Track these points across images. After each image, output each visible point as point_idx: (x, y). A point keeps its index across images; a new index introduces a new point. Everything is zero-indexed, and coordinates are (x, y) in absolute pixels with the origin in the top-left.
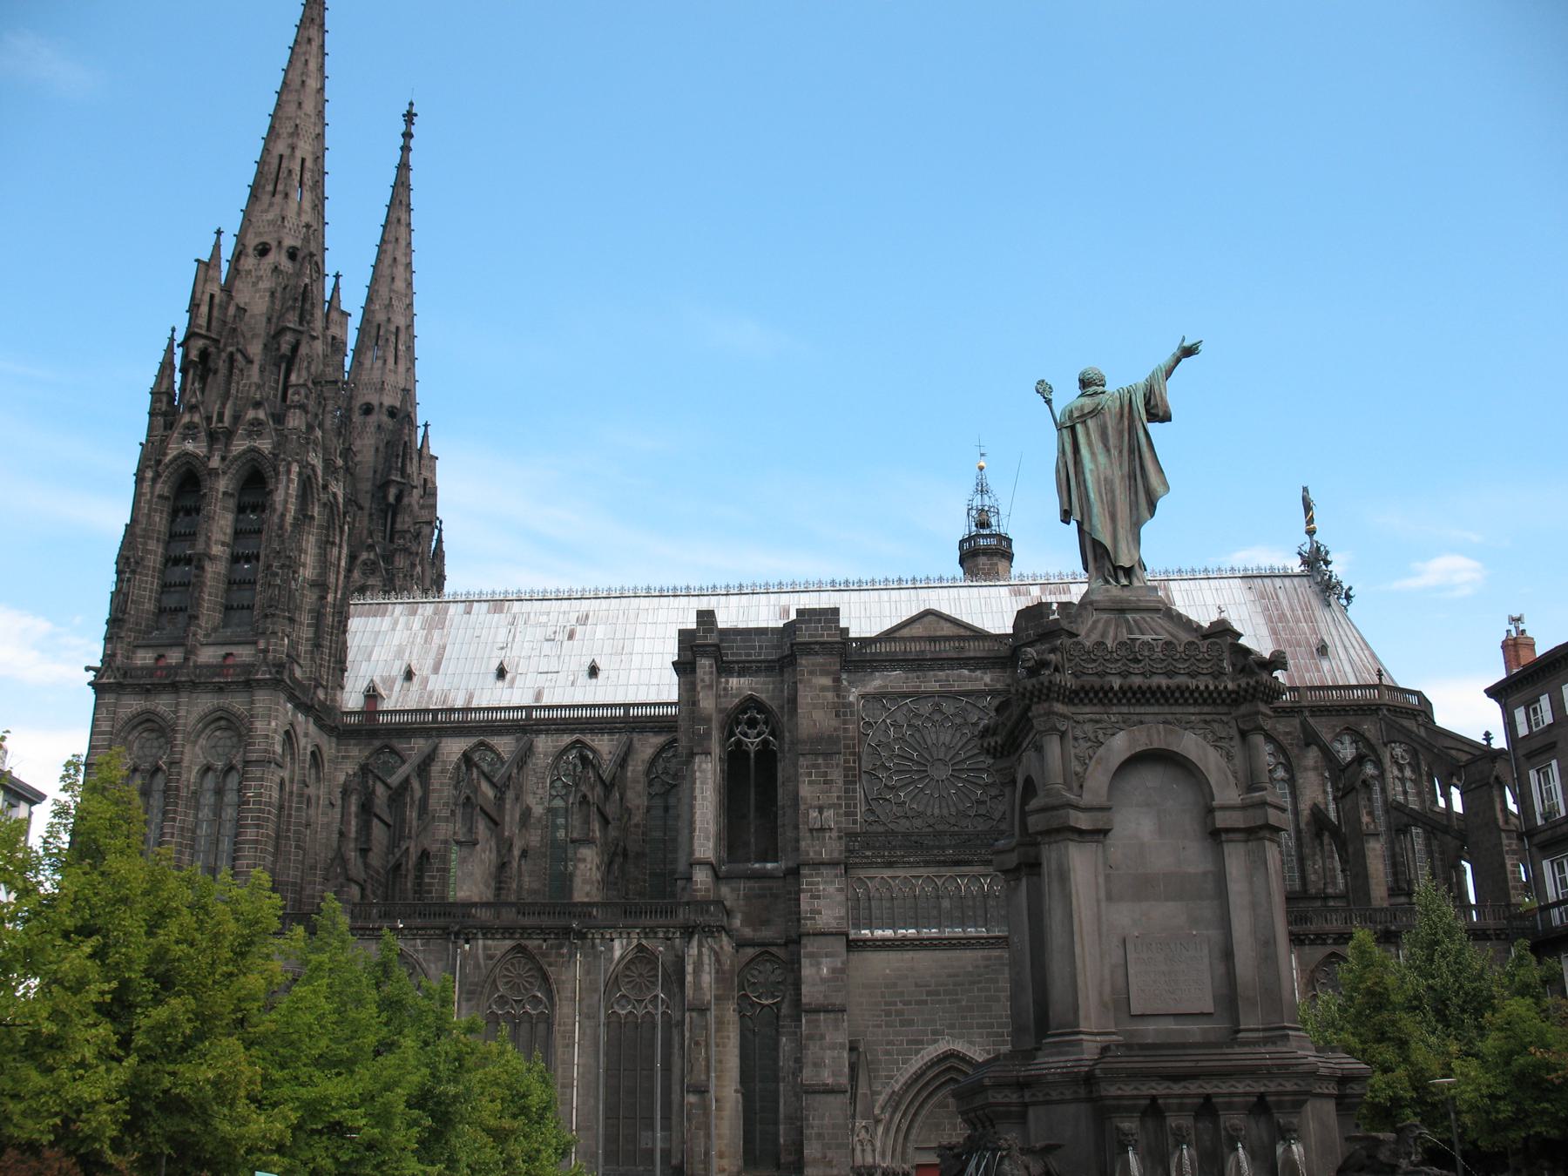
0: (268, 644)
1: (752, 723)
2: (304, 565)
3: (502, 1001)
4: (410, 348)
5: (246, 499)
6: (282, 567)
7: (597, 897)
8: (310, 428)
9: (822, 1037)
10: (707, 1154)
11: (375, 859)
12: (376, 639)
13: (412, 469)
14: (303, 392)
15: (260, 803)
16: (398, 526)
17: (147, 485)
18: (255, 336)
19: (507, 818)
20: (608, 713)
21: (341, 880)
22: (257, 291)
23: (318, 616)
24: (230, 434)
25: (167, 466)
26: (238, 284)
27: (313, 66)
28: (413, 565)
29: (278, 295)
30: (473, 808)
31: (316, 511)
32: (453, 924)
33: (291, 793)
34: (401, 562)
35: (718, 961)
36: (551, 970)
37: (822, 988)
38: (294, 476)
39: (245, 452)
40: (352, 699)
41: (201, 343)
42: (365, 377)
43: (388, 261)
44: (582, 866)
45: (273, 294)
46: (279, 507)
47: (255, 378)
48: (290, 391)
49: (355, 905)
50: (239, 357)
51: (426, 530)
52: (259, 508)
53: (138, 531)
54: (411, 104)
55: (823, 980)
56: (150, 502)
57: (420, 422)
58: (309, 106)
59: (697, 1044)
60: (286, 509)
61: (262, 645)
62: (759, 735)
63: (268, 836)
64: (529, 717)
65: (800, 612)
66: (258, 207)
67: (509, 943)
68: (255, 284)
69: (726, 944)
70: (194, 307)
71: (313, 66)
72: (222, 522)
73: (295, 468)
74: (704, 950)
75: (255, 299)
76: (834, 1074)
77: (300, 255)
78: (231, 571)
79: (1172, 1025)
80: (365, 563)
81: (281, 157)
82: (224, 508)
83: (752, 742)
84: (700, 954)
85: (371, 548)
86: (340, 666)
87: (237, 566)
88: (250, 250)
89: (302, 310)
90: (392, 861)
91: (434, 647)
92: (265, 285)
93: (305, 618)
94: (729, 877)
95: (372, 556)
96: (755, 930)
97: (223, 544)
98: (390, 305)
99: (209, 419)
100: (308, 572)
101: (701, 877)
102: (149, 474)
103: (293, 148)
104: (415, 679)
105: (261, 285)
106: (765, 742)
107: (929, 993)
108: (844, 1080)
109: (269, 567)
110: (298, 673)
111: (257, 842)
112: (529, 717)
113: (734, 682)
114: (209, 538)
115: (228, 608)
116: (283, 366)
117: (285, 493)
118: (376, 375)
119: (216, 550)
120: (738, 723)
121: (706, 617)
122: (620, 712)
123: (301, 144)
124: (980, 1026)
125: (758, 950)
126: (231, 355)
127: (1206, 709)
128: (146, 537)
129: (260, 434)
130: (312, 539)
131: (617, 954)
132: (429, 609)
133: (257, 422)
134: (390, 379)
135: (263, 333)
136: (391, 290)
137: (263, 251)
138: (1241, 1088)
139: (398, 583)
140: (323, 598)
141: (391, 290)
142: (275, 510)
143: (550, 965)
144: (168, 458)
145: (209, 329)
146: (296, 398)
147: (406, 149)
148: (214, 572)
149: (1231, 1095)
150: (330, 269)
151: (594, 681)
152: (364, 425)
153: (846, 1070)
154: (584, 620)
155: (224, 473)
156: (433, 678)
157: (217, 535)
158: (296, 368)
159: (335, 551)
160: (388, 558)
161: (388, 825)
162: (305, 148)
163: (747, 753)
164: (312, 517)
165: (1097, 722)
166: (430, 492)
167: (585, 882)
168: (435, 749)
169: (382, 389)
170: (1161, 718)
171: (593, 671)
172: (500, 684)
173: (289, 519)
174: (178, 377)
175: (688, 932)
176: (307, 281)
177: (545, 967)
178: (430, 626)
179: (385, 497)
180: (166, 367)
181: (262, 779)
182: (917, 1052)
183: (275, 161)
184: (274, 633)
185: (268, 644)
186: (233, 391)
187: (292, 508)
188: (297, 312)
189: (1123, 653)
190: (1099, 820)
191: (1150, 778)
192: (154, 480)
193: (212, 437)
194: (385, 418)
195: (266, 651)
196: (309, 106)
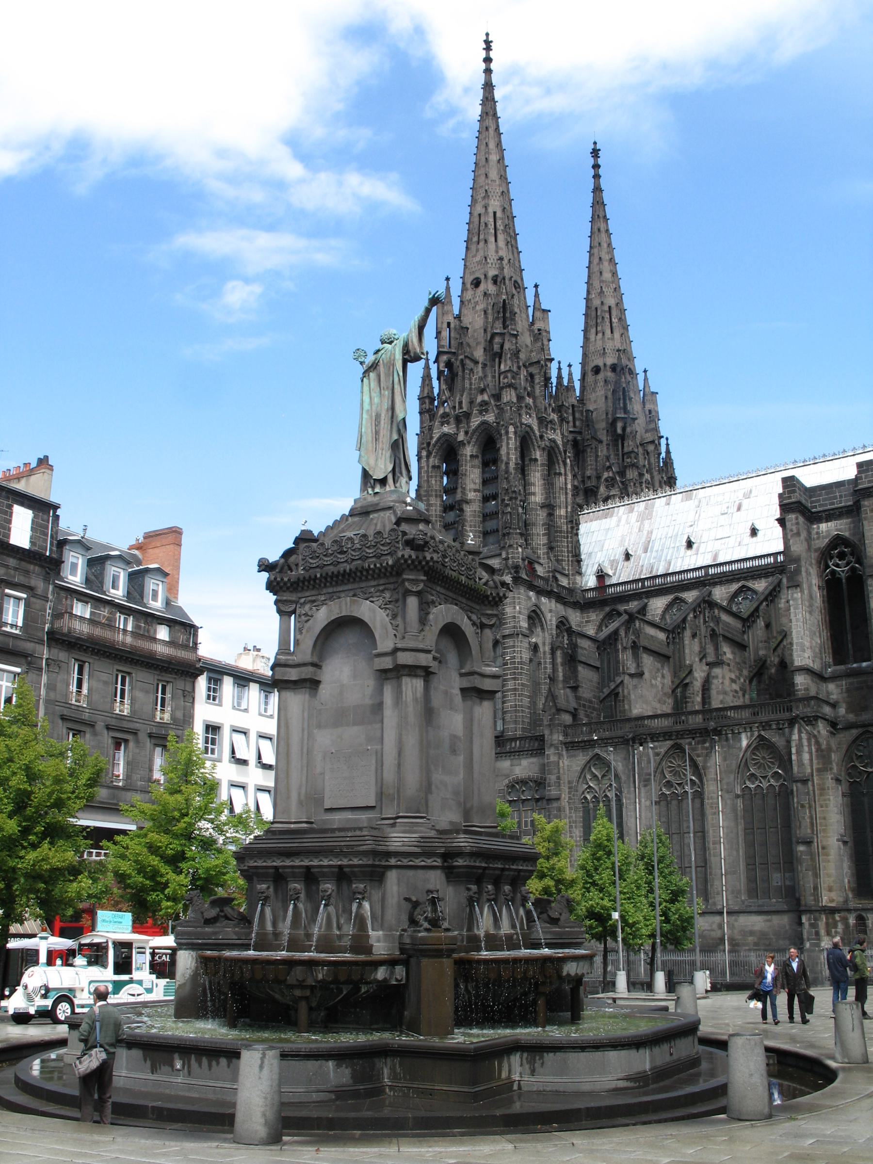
0: (508, 554)
1: (842, 556)
2: (534, 494)
3: (669, 784)
4: (622, 320)
5: (488, 457)
6: (511, 499)
7: (730, 701)
8: (520, 398)
10: (816, 888)
11: (586, 692)
12: (606, 534)
13: (636, 407)
14: (509, 375)
15: (514, 663)
16: (626, 450)
17: (424, 460)
18: (478, 344)
19: (687, 651)
20: (763, 562)
21: (553, 710)
22: (476, 312)
23: (551, 528)
24: (468, 415)
25: (434, 446)
26: (465, 311)
27: (492, 145)
28: (641, 475)
29: (490, 311)
30: (639, 649)
31: (538, 454)
32: (635, 734)
33: (544, 653)
34: (631, 474)
35: (817, 743)
36: (700, 760)
38: (512, 435)
39: (479, 426)
40: (590, 581)
41: (445, 358)
42: (592, 348)
43: (596, 261)
44: (715, 681)
45: (485, 312)
46: (504, 458)
47: (480, 374)
48: (502, 377)
49: (565, 726)
50: (468, 362)
51: (651, 448)
52: (495, 461)
53: (423, 493)
54: (595, 143)
56: (427, 472)
57: (639, 369)
58: (494, 174)
59: (803, 806)
60: (508, 459)
61: (504, 556)
62: (848, 564)
63: (523, 684)
64: (707, 574)
65: (860, 465)
66: (470, 255)
67: (669, 743)
68: (474, 308)
69: (822, 728)
71: (492, 145)
72: (472, 476)
73: (511, 429)
74: (804, 736)
75: (475, 321)
77: (499, 280)
78: (483, 508)
79: (349, 815)
80: (606, 480)
81: (480, 215)
82: (473, 466)
83: (842, 570)
84: (800, 738)
85: (609, 468)
86: (577, 559)
87: (488, 504)
88: (468, 286)
89: (504, 317)
90: (606, 691)
91: (645, 533)
92: (480, 307)
93: (541, 530)
94: (833, 678)
95: (611, 474)
96: (856, 715)
97: (475, 491)
98: (602, 292)
99: (454, 407)
100: (538, 496)
101: (800, 680)
102: (424, 453)
103: (486, 208)
104: (632, 559)
105: (478, 308)
106: (853, 569)
109: (503, 500)
110: (540, 571)
111: (515, 689)
112: (707, 574)
113: (823, 526)
114: (464, 489)
115: (485, 534)
116: (497, 360)
117: (509, 449)
118: (599, 343)
119: (471, 495)
120: (831, 558)
121: (790, 483)
122: (771, 560)
123: (492, 202)
125: (860, 730)
126: (462, 360)
127: (382, 581)
128: (428, 495)
129: (487, 411)
130: (538, 475)
131: (744, 743)
132: (642, 505)
133: (484, 403)
134: (609, 345)
135: (483, 341)
136: (601, 281)
137: (477, 283)
138: (325, 862)
139: (630, 490)
140: (550, 515)
141: (601, 281)
142: (502, 461)
143: (698, 756)
144: (434, 440)
145: (450, 347)
146: (506, 381)
147: (597, 177)
148: (471, 511)
149: (293, 867)
150: (528, 282)
151: (755, 539)
152: (596, 382)
154: (748, 495)
155: (469, 443)
156: (643, 555)
157: (470, 486)
158: (503, 361)
159: (562, 479)
160: (622, 474)
161: (597, 668)
162: (495, 204)
163: (840, 579)
164: (536, 460)
165: (314, 601)
166: (652, 417)
167: (718, 693)
168: (646, 605)
169: (604, 353)
170: (351, 593)
171: (754, 532)
172: (689, 552)
173: (512, 465)
174: (435, 383)
175: (792, 722)
176: (504, 297)
177: (695, 758)
178: (642, 518)
179: (615, 430)
181: (514, 647)
183: (476, 220)
184: (510, 546)
185: (508, 554)
186: (467, 385)
187: (513, 457)
188: (501, 320)
189: (335, 548)
190: (307, 672)
191: (350, 638)
192: (428, 457)
193: (458, 420)
194: (610, 374)
195: (507, 559)
196: (494, 174)
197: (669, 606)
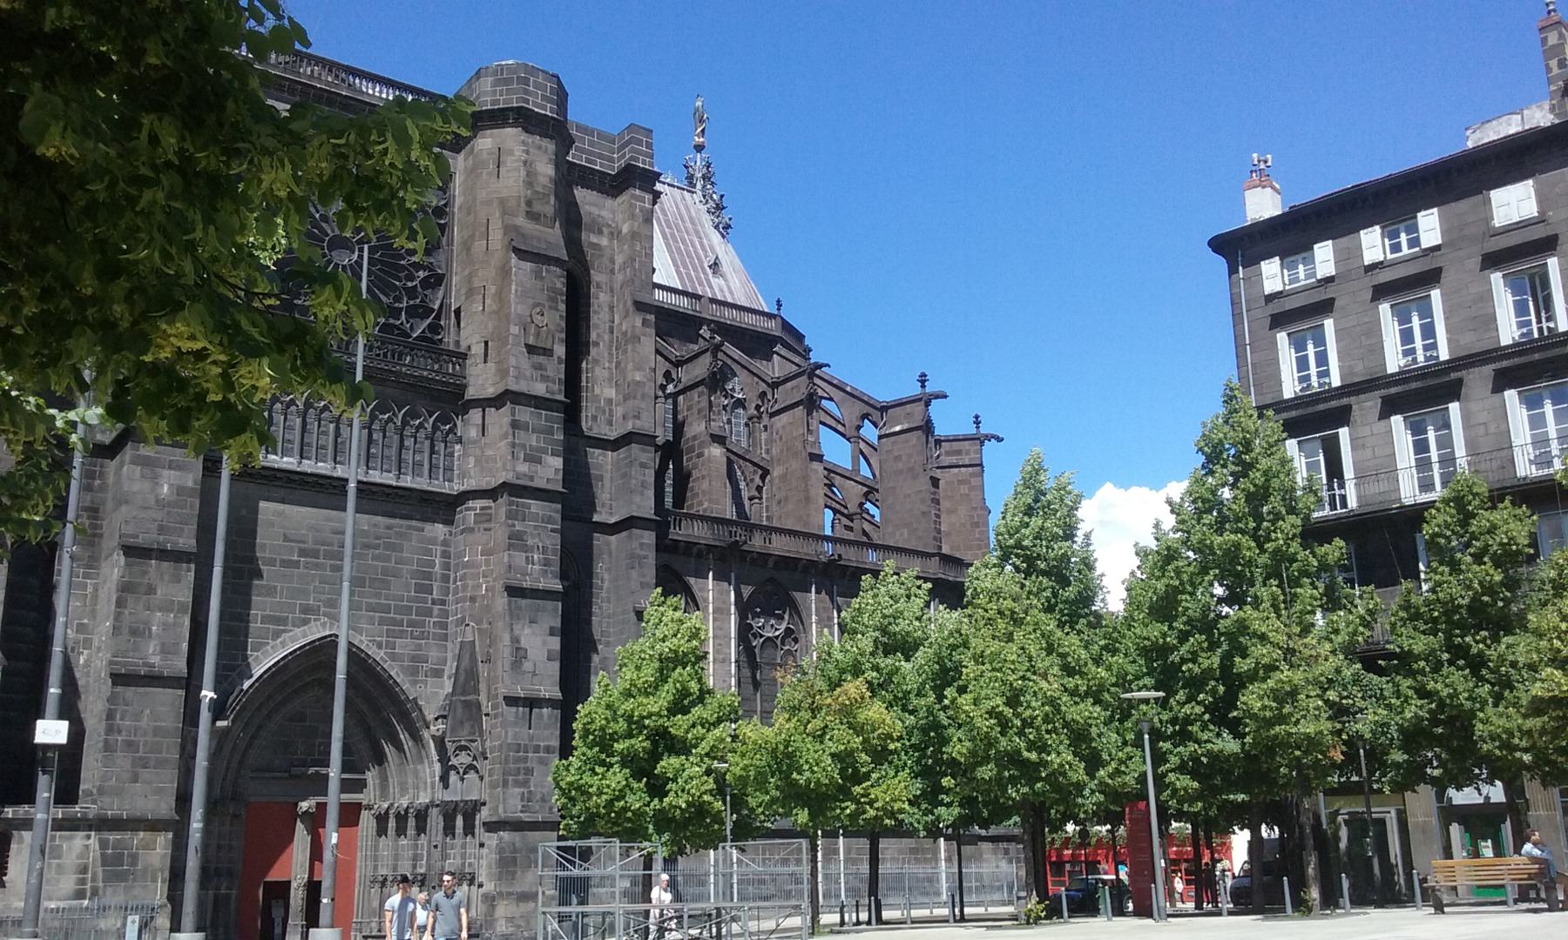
9: (151, 590)
37: (159, 515)
55: (161, 504)
76: (165, 651)
107: (303, 553)
108: (180, 665)
124: (371, 608)
153: (185, 646)
182: (277, 635)
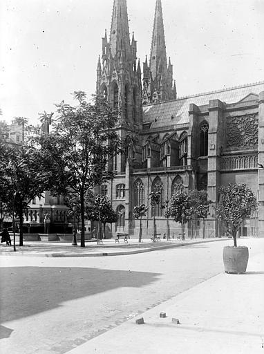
51: (168, 84)
70: (103, 49)
75: (114, 46)
180: (99, 64)
197: (165, 136)
